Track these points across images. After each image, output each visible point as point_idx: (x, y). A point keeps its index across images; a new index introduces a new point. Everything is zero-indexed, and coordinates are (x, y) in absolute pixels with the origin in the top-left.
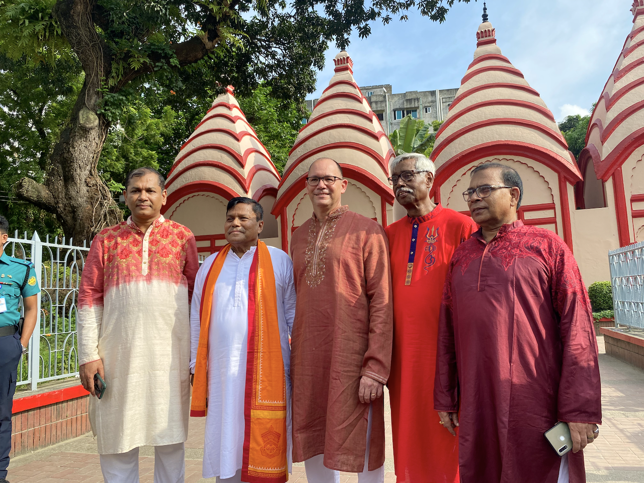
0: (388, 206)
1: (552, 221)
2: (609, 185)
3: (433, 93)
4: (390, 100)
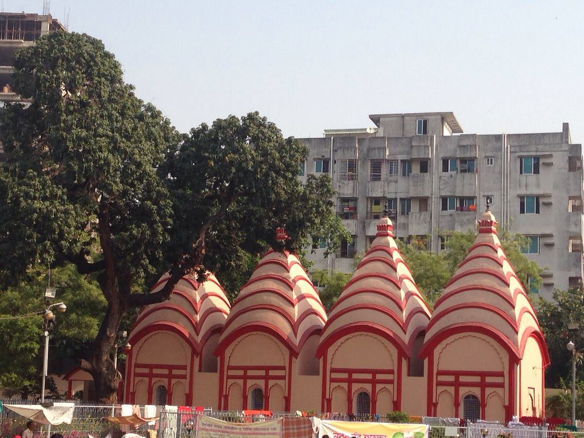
0: (294, 359)
1: (391, 382)
2: (426, 361)
3: (498, 138)
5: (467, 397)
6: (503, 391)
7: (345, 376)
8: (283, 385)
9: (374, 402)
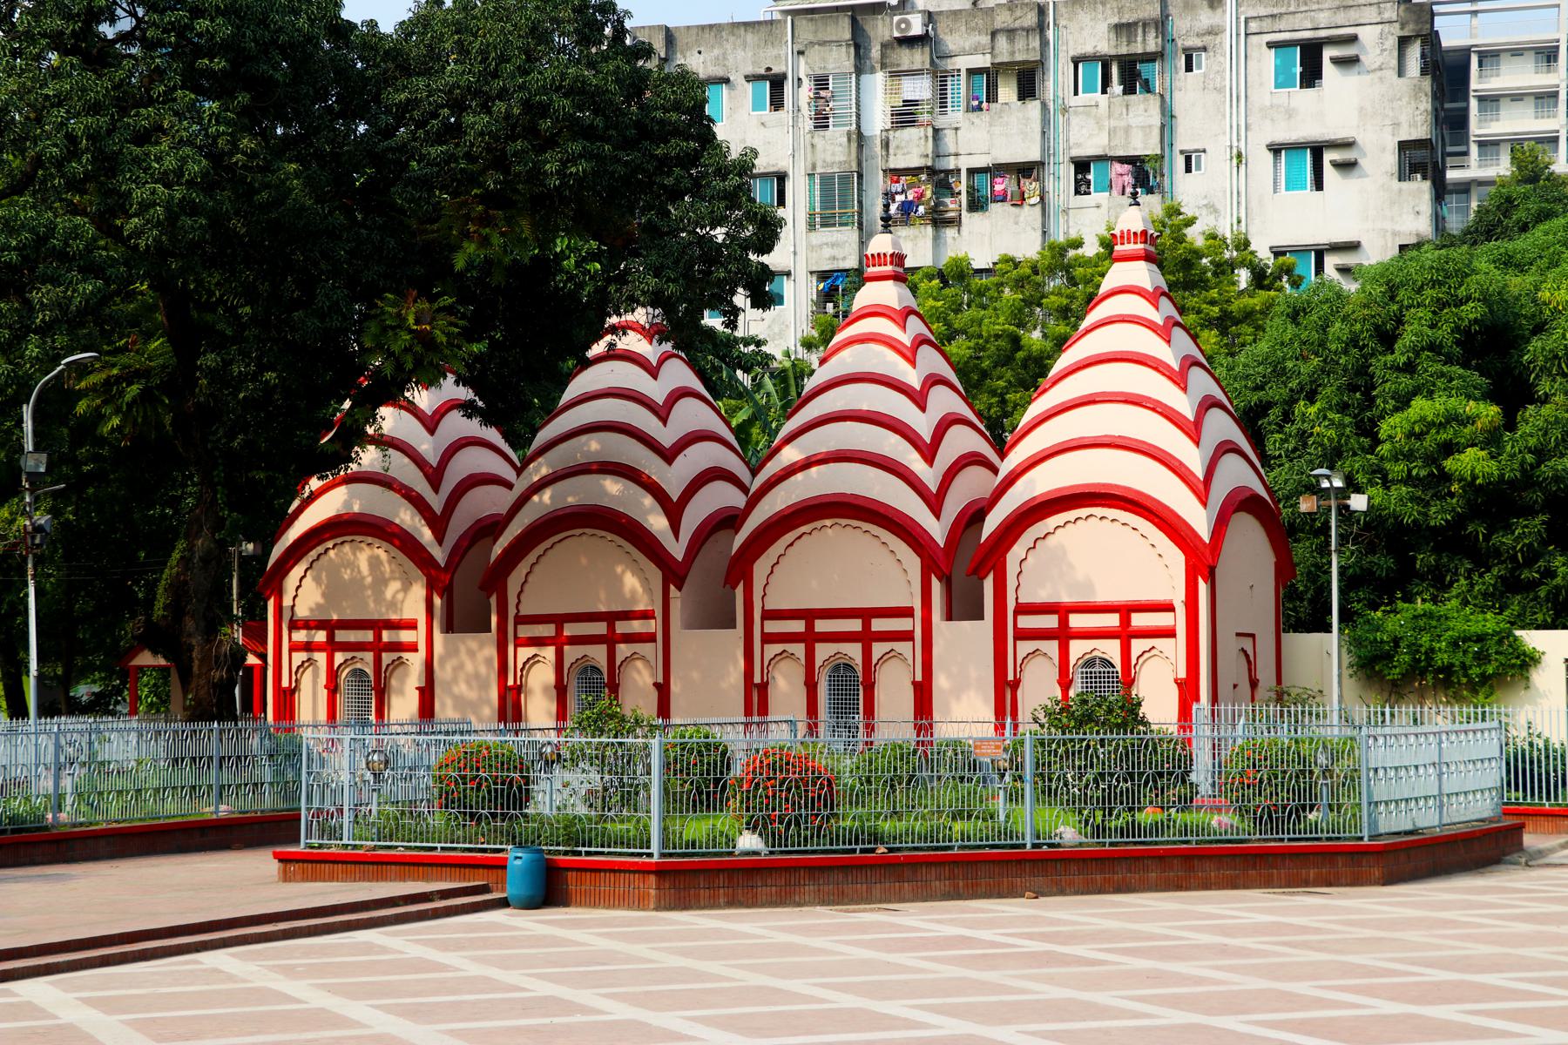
4: (1062, 22)
5: (1090, 663)
6: (491, 652)
7: (798, 626)
8: (651, 657)
9: (870, 687)
